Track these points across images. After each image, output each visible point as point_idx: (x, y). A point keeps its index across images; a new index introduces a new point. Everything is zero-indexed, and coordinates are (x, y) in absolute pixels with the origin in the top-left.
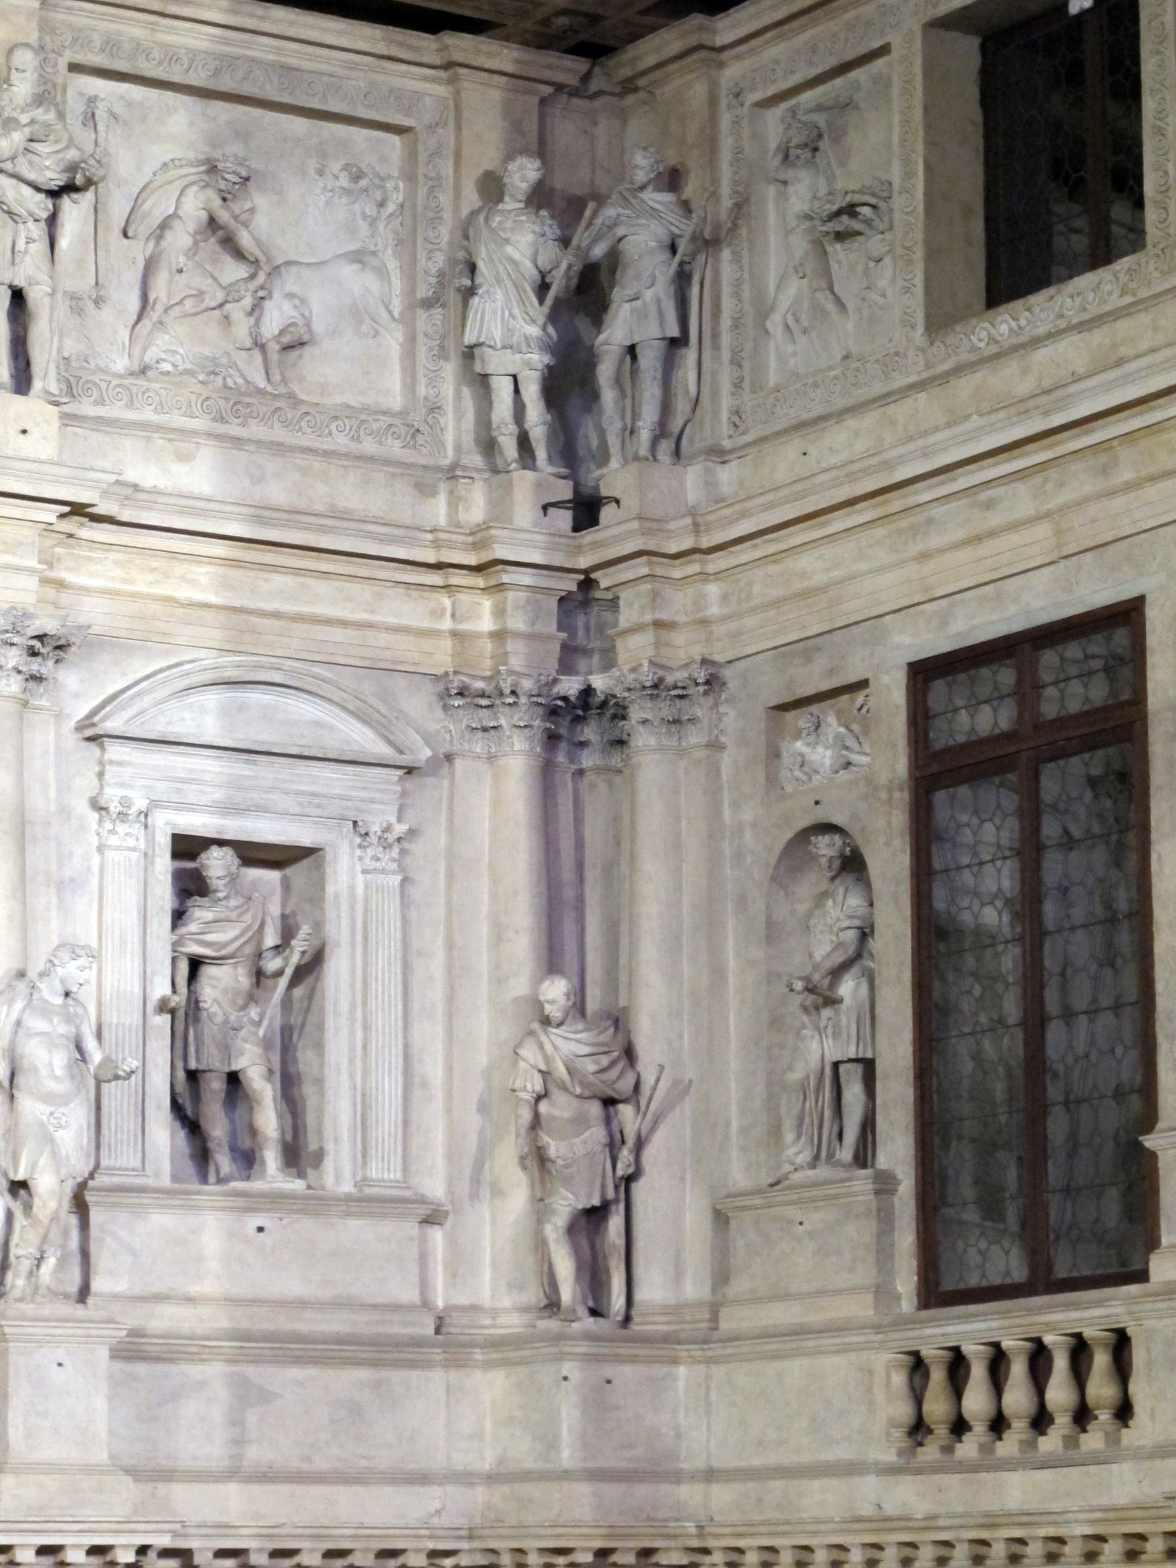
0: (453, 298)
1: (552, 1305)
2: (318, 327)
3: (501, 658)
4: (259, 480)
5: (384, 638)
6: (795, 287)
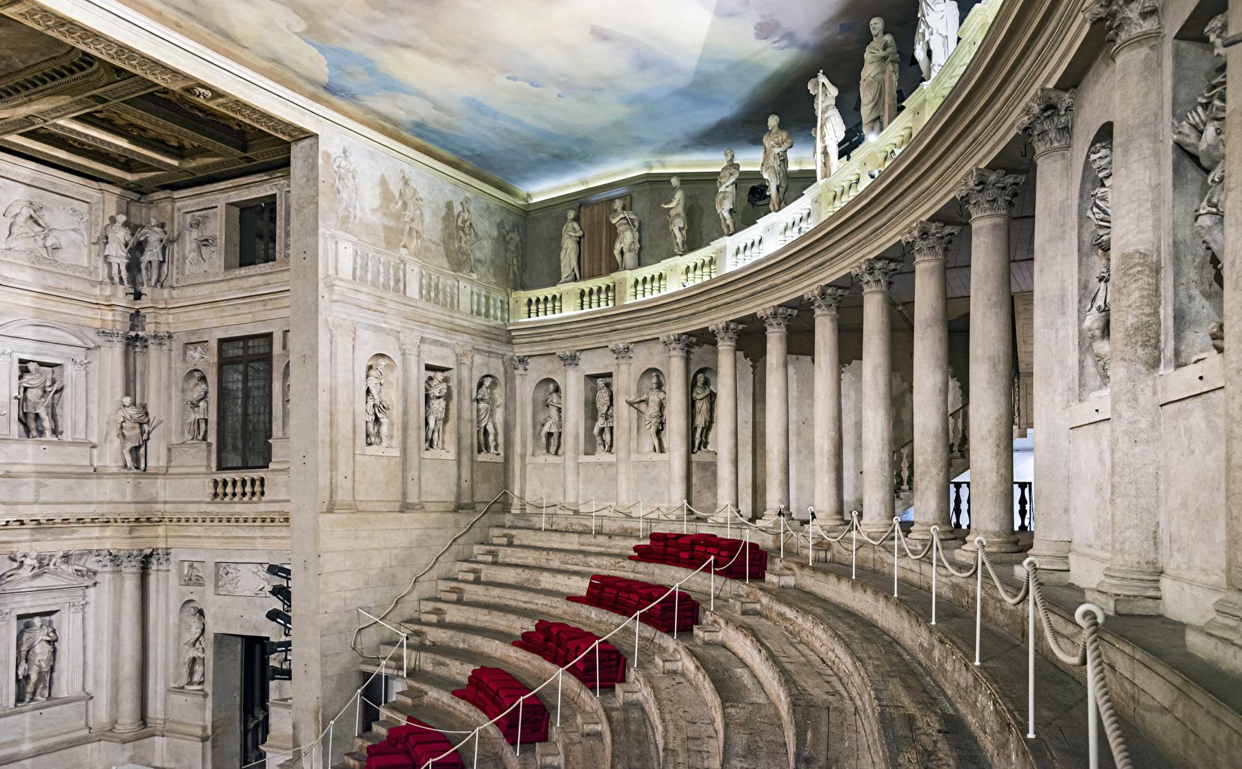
0: (102, 245)
1: (125, 466)
2: (63, 245)
3: (114, 326)
4: (45, 278)
5: (82, 319)
6: (193, 254)
